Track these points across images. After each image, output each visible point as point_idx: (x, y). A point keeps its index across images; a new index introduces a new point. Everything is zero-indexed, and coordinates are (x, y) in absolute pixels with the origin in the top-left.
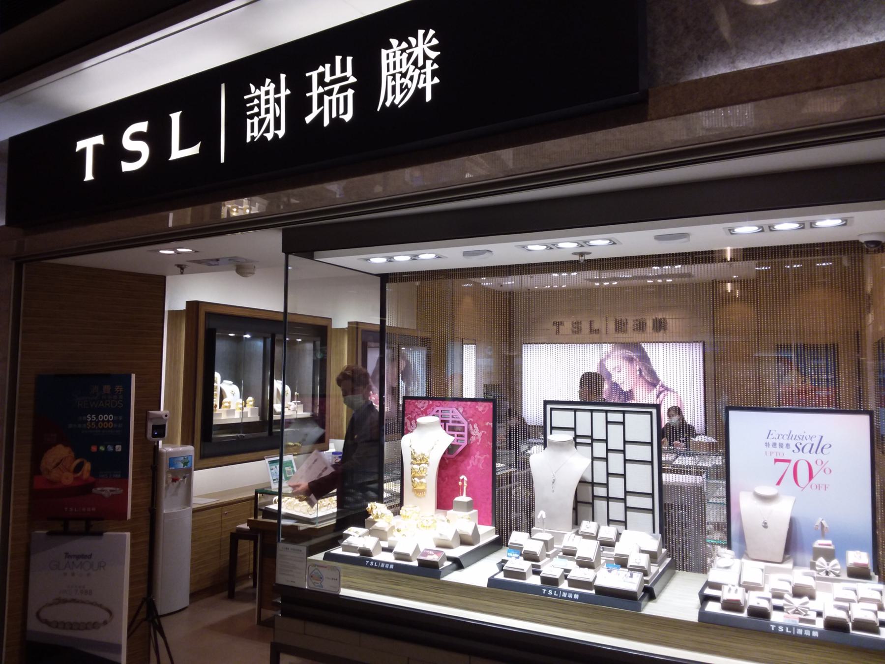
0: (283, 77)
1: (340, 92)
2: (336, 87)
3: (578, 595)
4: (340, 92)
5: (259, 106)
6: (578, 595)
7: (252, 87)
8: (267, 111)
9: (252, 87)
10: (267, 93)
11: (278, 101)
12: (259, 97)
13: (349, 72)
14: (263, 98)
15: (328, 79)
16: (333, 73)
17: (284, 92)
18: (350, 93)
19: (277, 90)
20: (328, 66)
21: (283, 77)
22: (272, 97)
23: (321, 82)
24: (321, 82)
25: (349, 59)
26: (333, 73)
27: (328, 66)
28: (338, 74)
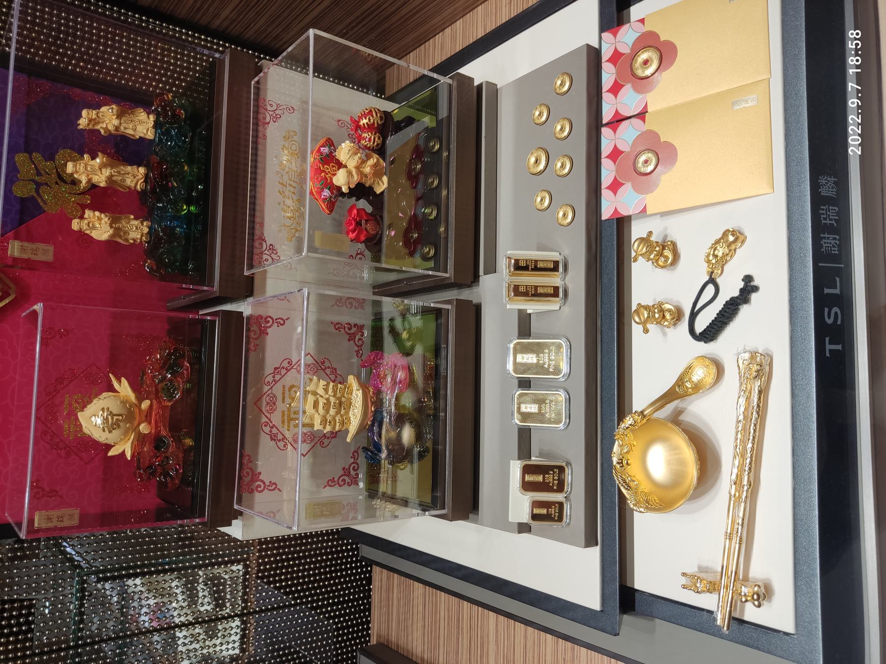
0: (822, 235)
1: (829, 212)
2: (828, 213)
3: (822, 180)
4: (829, 212)
5: (828, 247)
6: (822, 180)
7: (823, 250)
8: (830, 243)
9: (823, 250)
10: (825, 243)
11: (828, 238)
12: (826, 247)
13: (825, 208)
14: (827, 245)
15: (825, 216)
16: (823, 214)
17: (826, 235)
18: (830, 208)
19: (825, 238)
20: (822, 216)
21: (822, 235)
22: (826, 241)
23: (825, 219)
24: (825, 219)
25: (821, 207)
26: (823, 214)
27: (822, 216)
28: (824, 212)
